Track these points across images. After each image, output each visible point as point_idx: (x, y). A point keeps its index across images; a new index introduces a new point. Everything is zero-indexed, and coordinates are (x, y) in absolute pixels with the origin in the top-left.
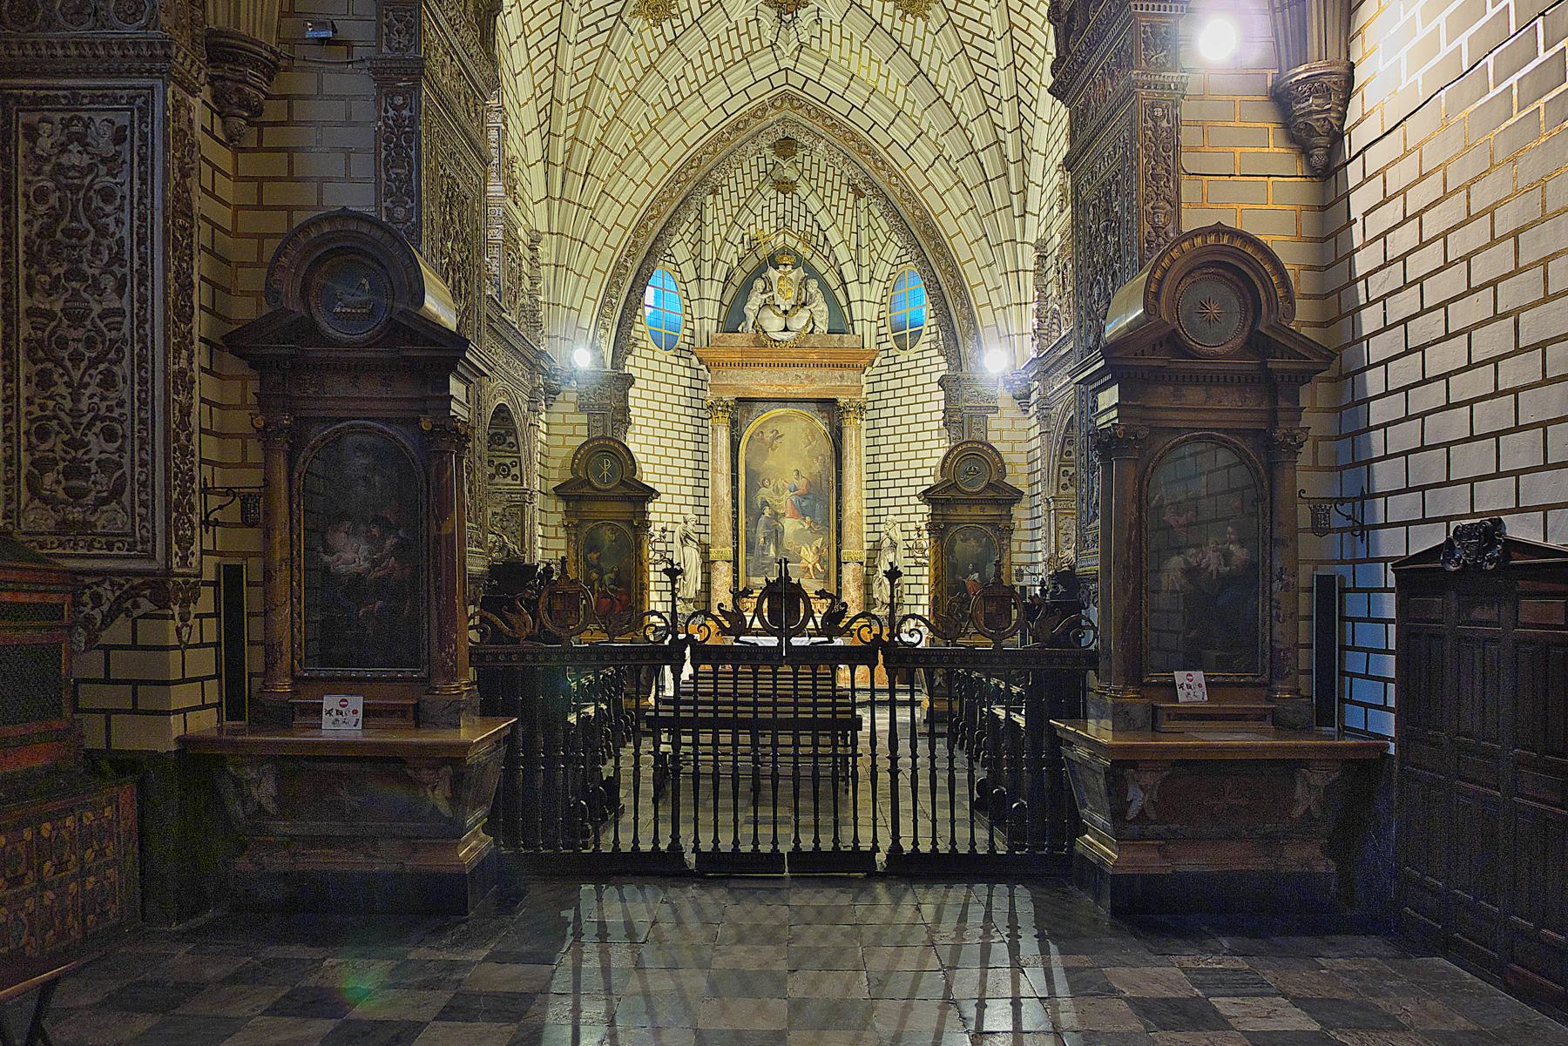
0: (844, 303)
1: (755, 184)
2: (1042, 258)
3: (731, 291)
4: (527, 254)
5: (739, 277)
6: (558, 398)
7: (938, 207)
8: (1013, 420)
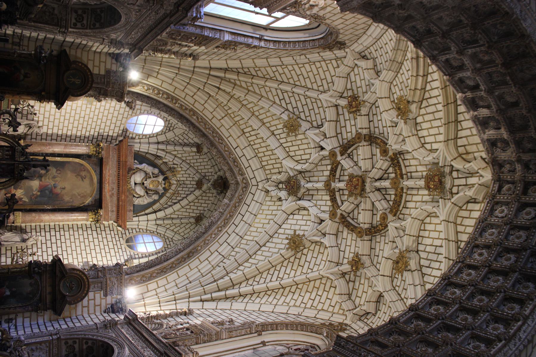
0: (147, 212)
1: (200, 171)
2: (185, 314)
3: (152, 158)
4: (189, 52)
5: (159, 162)
6: (114, 61)
7: (202, 258)
8: (100, 305)
